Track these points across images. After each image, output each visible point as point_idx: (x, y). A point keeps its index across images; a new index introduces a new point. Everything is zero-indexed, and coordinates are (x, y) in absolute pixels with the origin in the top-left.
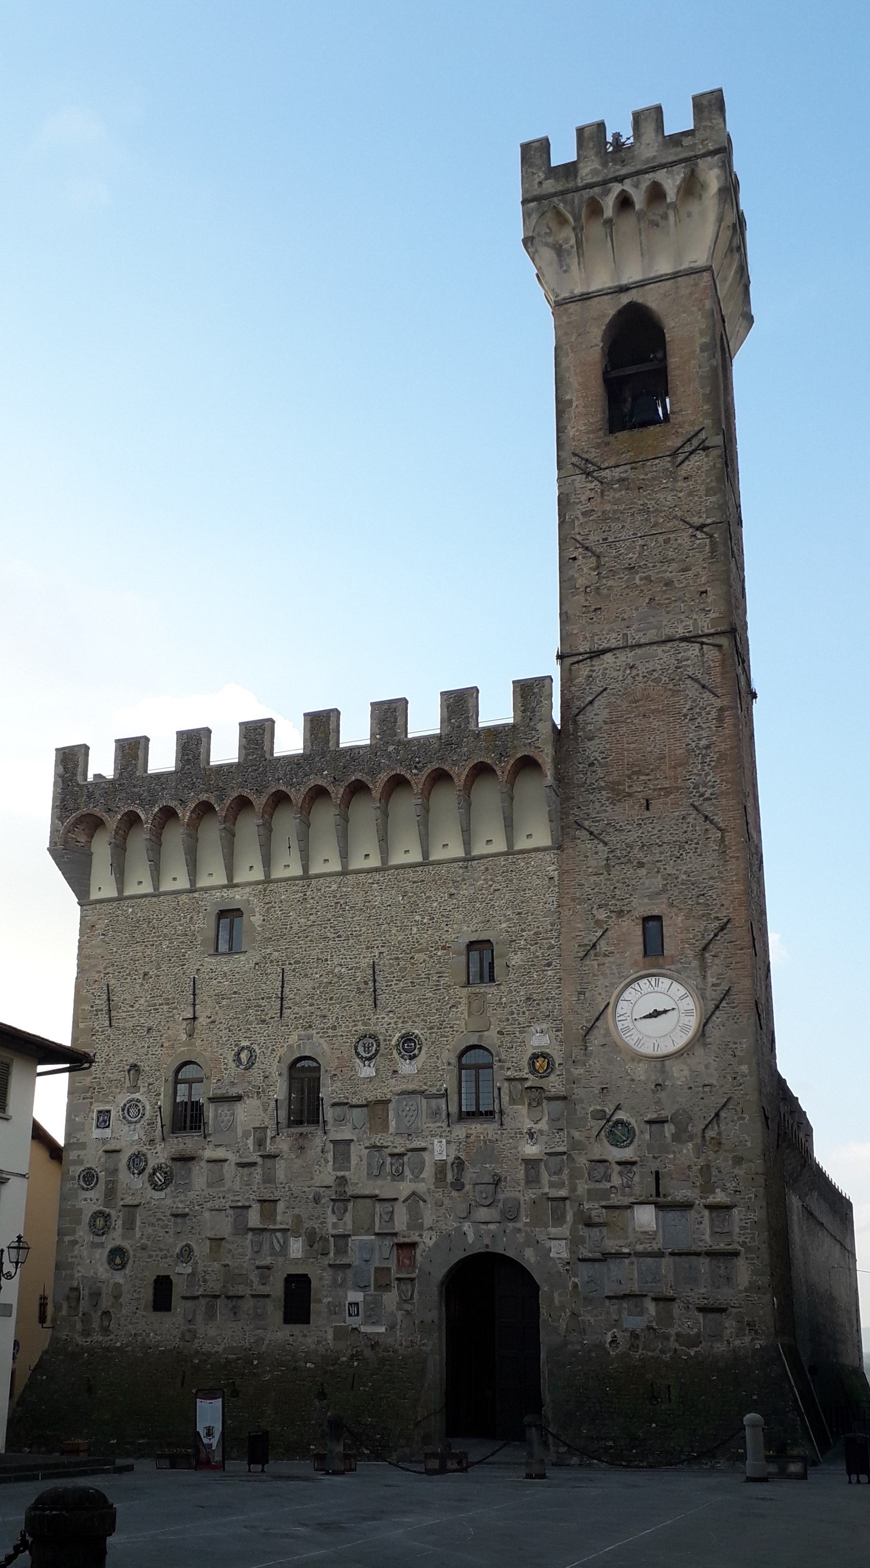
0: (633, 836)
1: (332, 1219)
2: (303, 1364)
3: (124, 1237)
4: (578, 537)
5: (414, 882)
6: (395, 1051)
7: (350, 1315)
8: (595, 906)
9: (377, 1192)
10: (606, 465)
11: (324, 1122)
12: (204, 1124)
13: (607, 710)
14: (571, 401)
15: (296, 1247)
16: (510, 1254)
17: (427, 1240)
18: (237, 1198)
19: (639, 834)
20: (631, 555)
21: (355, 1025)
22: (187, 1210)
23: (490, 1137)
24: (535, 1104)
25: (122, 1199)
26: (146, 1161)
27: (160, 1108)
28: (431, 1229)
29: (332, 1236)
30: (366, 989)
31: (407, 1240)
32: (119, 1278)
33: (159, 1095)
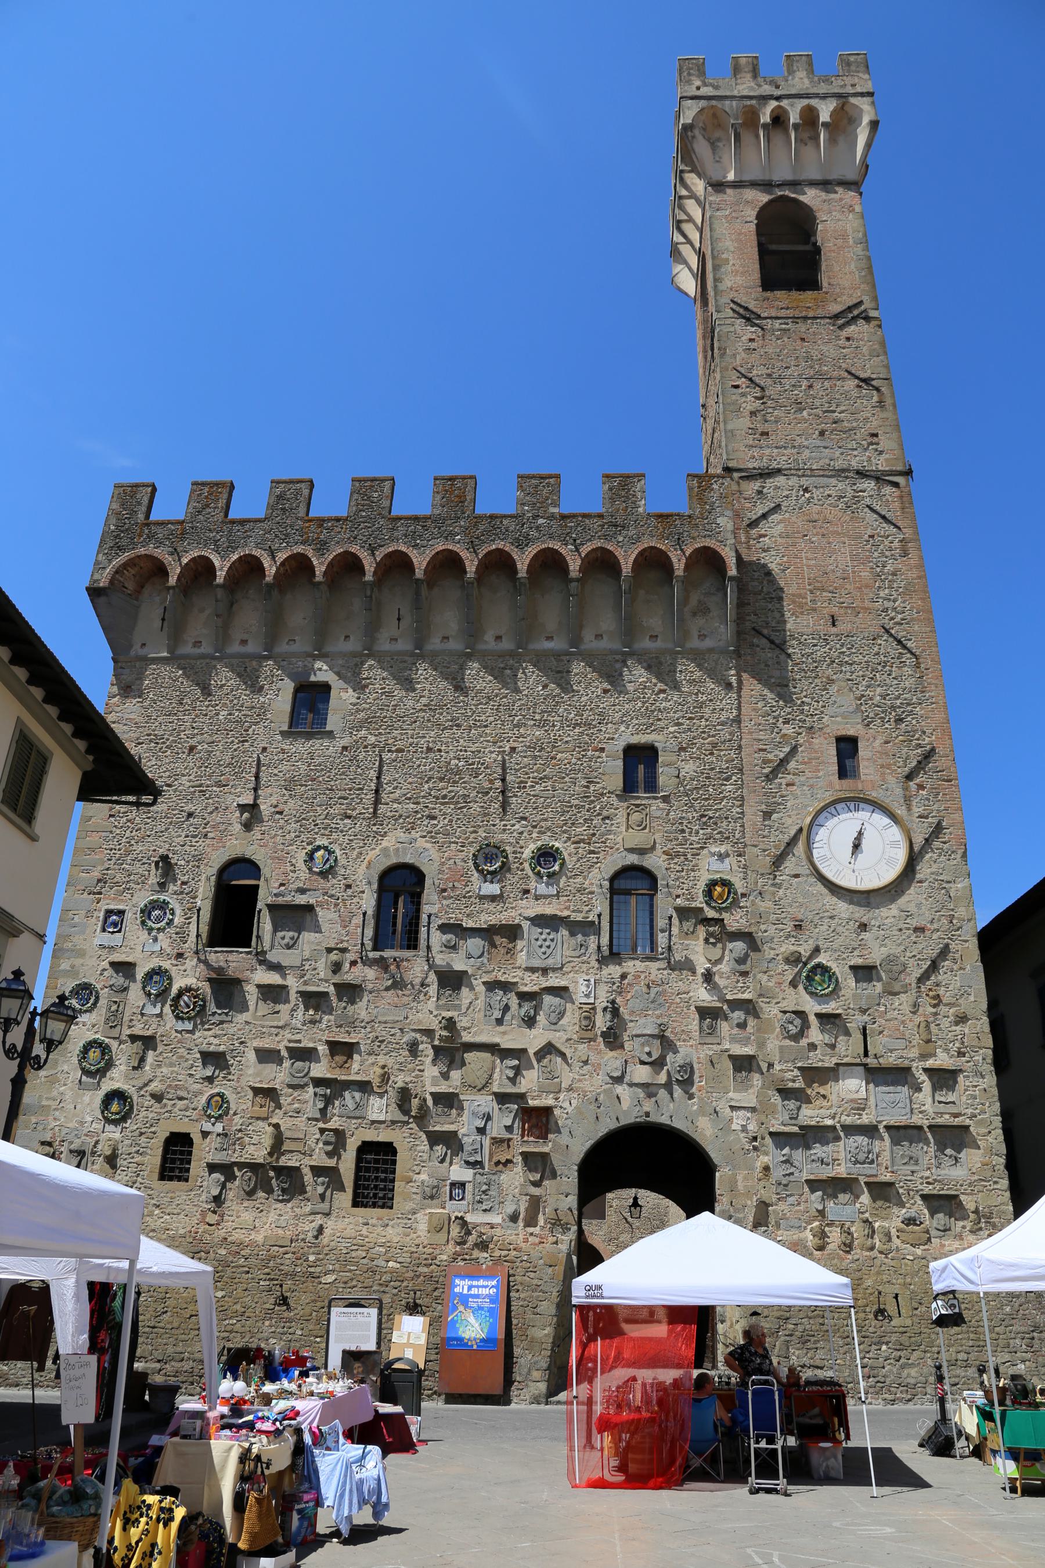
0: (820, 652)
1: (431, 1071)
2: (383, 1264)
3: (127, 1078)
4: (739, 368)
5: (559, 672)
6: (526, 865)
7: (451, 1198)
8: (781, 720)
9: (496, 1040)
10: (766, 315)
12: (258, 937)
13: (782, 525)
14: (727, 260)
15: (378, 1108)
16: (679, 1124)
17: (566, 1105)
18: (297, 1037)
19: (826, 649)
20: (796, 392)
21: (475, 832)
22: (222, 1048)
23: (652, 977)
24: (712, 940)
25: (130, 1027)
26: (170, 978)
27: (199, 911)
28: (570, 1089)
29: (431, 1094)
30: (491, 789)
32: (114, 1133)
33: (194, 898)
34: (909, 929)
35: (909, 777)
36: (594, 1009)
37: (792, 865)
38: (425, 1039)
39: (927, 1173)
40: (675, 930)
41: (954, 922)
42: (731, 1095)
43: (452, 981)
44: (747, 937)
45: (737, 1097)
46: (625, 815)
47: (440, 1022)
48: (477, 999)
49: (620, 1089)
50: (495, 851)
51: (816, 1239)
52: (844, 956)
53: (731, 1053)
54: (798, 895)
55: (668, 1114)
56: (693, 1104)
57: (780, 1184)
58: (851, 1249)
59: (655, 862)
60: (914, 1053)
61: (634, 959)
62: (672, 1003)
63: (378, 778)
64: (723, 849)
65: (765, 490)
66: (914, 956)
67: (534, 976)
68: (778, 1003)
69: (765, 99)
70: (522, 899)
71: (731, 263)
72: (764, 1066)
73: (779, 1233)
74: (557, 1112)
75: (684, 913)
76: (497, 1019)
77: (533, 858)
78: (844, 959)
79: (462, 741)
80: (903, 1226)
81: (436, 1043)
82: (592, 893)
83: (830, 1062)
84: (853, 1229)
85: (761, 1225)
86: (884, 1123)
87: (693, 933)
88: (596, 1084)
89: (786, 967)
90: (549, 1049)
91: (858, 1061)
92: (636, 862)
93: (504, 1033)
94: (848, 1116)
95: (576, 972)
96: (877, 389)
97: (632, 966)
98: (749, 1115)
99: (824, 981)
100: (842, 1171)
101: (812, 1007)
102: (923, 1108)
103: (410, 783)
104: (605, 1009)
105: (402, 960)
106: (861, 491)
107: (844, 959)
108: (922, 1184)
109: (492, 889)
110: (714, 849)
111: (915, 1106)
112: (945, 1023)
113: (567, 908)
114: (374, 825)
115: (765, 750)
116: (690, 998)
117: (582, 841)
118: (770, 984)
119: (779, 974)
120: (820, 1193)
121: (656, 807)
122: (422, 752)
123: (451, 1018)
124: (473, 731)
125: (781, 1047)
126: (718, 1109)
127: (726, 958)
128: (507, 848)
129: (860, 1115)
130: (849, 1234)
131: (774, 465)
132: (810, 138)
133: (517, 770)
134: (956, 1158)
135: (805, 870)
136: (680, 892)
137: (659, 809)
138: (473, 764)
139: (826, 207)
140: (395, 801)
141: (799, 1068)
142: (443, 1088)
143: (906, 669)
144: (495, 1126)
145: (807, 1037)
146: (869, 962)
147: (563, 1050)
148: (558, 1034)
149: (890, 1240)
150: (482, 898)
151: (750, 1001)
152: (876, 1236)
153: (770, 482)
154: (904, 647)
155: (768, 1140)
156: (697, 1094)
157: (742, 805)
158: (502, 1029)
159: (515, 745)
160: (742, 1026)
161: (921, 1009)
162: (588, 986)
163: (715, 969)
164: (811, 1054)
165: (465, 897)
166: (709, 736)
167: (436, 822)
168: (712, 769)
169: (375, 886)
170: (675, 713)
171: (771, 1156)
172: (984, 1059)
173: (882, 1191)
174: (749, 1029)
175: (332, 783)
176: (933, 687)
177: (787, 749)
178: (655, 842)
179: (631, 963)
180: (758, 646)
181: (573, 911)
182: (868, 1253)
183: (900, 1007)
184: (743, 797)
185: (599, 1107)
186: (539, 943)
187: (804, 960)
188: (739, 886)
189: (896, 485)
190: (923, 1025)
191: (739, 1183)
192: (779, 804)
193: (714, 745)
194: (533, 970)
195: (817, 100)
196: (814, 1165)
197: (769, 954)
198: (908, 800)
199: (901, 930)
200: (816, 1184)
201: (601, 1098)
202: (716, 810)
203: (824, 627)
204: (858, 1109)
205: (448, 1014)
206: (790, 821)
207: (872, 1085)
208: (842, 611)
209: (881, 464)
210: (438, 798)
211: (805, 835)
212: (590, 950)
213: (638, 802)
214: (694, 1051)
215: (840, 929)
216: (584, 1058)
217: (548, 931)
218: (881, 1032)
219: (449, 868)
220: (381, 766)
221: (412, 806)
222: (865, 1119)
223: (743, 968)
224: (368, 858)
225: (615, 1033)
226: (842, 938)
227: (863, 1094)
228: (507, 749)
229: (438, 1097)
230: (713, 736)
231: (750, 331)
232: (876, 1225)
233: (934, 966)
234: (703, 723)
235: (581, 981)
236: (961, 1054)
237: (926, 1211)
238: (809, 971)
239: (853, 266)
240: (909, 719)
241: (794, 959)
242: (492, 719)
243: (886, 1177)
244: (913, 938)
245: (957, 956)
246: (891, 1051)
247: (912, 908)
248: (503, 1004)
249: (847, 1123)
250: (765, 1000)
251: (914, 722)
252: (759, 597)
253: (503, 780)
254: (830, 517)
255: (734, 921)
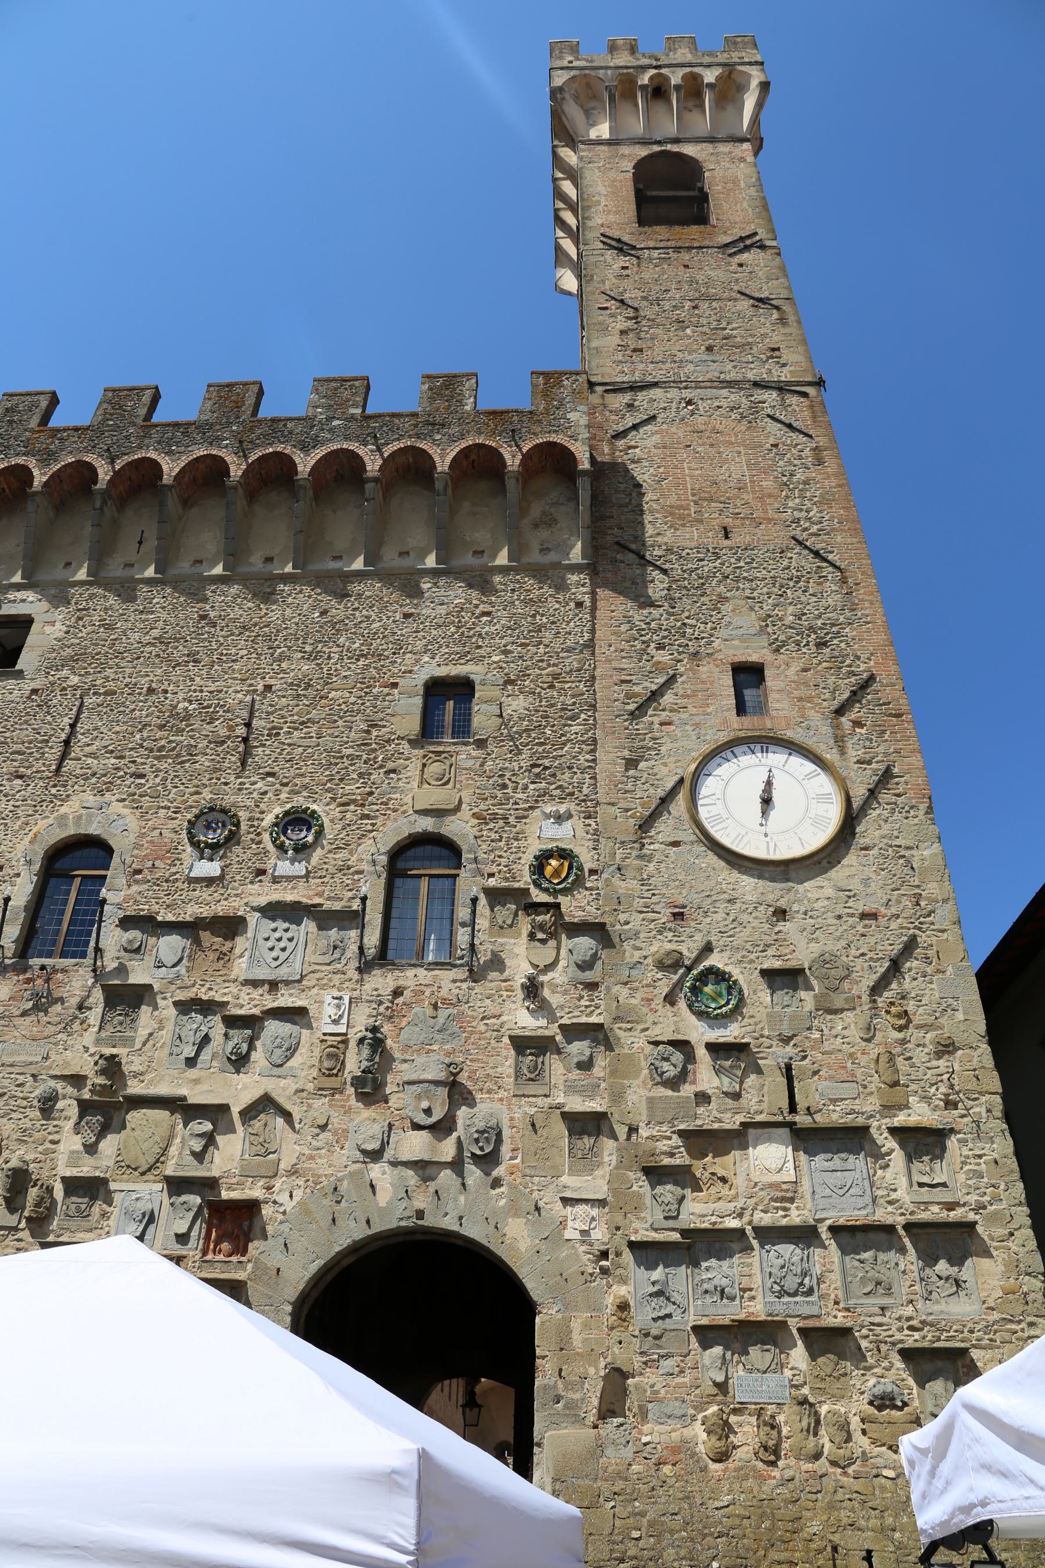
0: (708, 566)
1: (71, 1142)
4: (608, 292)
6: (266, 837)
8: (653, 645)
9: (183, 1091)
11: (98, 950)
14: (598, 203)
16: (474, 1231)
17: (283, 1198)
21: (197, 793)
23: (444, 993)
24: (540, 935)
28: (293, 1172)
29: (64, 1179)
31: (235, 1195)
34: (852, 915)
35: (840, 711)
36: (345, 1042)
37: (669, 829)
38: (70, 1090)
39: (909, 1311)
40: (483, 923)
41: (923, 903)
42: (565, 1179)
43: (126, 998)
44: (597, 930)
45: (574, 1183)
46: (420, 767)
47: (96, 1063)
48: (160, 1029)
49: (377, 1171)
50: (222, 817)
51: (714, 1438)
52: (752, 956)
53: (566, 1109)
54: (678, 870)
55: (453, 1214)
56: (500, 1196)
57: (647, 1335)
58: (778, 1458)
59: (460, 828)
60: (871, 1104)
61: (415, 966)
62: (472, 1033)
63: (73, 726)
64: (562, 809)
65: (636, 403)
66: (863, 955)
67: (256, 993)
68: (647, 1029)
69: (644, 68)
70: (252, 883)
71: (603, 204)
72: (622, 1131)
73: (646, 1428)
74: (266, 1211)
75: (496, 896)
76: (187, 1059)
77: (276, 825)
78: (752, 961)
79: (197, 679)
80: (872, 1410)
81: (86, 1095)
82: (361, 872)
83: (732, 1122)
84: (781, 1418)
85: (613, 1414)
86: (828, 1222)
87: (511, 926)
88: (338, 1162)
89: (659, 975)
90: (265, 1104)
91: (780, 1119)
92: (430, 829)
93: (197, 1081)
94: (765, 1212)
95: (323, 987)
96: (777, 308)
97: (412, 977)
98: (595, 1212)
99: (720, 995)
100: (757, 1309)
101: (701, 1034)
102: (893, 1196)
103: (117, 733)
104: (361, 1041)
105: (55, 971)
106: (760, 402)
107: (752, 961)
108: (900, 1330)
109: (210, 868)
110: (549, 809)
111: (879, 1193)
112: (920, 1056)
113: (320, 895)
114: (55, 786)
115: (630, 681)
116: (502, 1025)
117: (354, 801)
118: (633, 1001)
119: (648, 986)
120: (718, 1350)
121: (466, 755)
122: (140, 694)
123: (114, 1056)
124: (216, 667)
125: (651, 1101)
126: (541, 1204)
127: (562, 963)
128: (240, 814)
129: (785, 1209)
130: (773, 1427)
131: (649, 379)
132: (696, 106)
133: (268, 713)
134: (956, 1281)
135: (687, 834)
136: (494, 869)
137: (470, 757)
138: (209, 707)
139: (713, 158)
140: (92, 755)
141: (681, 1133)
142: (86, 1169)
143: (828, 584)
144: (160, 1234)
145: (694, 1082)
146: (792, 964)
147: (288, 1107)
148: (283, 1082)
149: (849, 1439)
150: (191, 881)
151: (600, 1026)
152: (822, 1432)
153: (641, 396)
154: (826, 560)
155: (628, 1257)
156: (507, 1179)
157: (593, 751)
158: (193, 1073)
159: (272, 682)
160: (586, 1066)
161: (879, 1036)
162: (338, 1007)
163: (541, 978)
164: (701, 1110)
165: (167, 881)
166: (549, 665)
167: (143, 781)
168: (552, 705)
169: (37, 867)
170: (502, 638)
171: (635, 1282)
172: (989, 1111)
173: (829, 1341)
174: (597, 1071)
175: (7, 735)
176: (867, 604)
177: (661, 680)
178: (460, 801)
179: (410, 973)
180: (622, 562)
181: (329, 899)
182: (809, 1466)
183: (846, 1033)
184: (595, 740)
185: (338, 1202)
186: (270, 944)
187: (687, 962)
188: (587, 859)
189: (805, 395)
190: (884, 1059)
191: (575, 1336)
192: (649, 749)
193: (556, 676)
194: (255, 983)
195: (700, 68)
196: (709, 1299)
197: (632, 955)
198: (840, 742)
199: (839, 917)
200: (711, 1335)
201: (344, 1187)
202: (555, 758)
203: (713, 539)
204: (783, 1199)
205: (108, 1051)
206: (666, 772)
207: (802, 1156)
208: (738, 522)
209: (785, 375)
210: (151, 750)
211: (689, 786)
212: (349, 954)
213: (441, 749)
214: (504, 1108)
215: (744, 917)
216: (322, 1121)
217: (286, 925)
218: (816, 1073)
219: (151, 842)
220: (79, 712)
221: (113, 761)
222: (796, 1217)
223: (589, 976)
224: (35, 829)
225: (375, 1080)
226: (748, 930)
227: (789, 1175)
228: (260, 688)
229: (74, 1186)
230: (554, 665)
231: (623, 261)
232: (823, 1410)
233: (895, 967)
234: (542, 650)
235: (328, 999)
236: (950, 1104)
237: (911, 1382)
238: (696, 979)
239: (745, 204)
240: (835, 642)
241: (671, 963)
242: (245, 652)
243: (838, 1319)
244: (860, 928)
245: (931, 953)
246: (834, 1101)
247: (855, 885)
248: (200, 1035)
249: (763, 1224)
250: (624, 1025)
251: (843, 645)
252: (626, 510)
253: (248, 725)
254: (721, 428)
255: (576, 907)
